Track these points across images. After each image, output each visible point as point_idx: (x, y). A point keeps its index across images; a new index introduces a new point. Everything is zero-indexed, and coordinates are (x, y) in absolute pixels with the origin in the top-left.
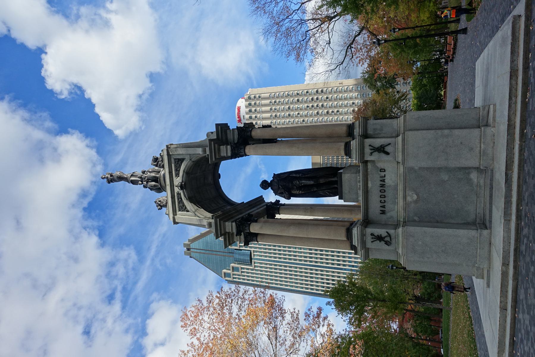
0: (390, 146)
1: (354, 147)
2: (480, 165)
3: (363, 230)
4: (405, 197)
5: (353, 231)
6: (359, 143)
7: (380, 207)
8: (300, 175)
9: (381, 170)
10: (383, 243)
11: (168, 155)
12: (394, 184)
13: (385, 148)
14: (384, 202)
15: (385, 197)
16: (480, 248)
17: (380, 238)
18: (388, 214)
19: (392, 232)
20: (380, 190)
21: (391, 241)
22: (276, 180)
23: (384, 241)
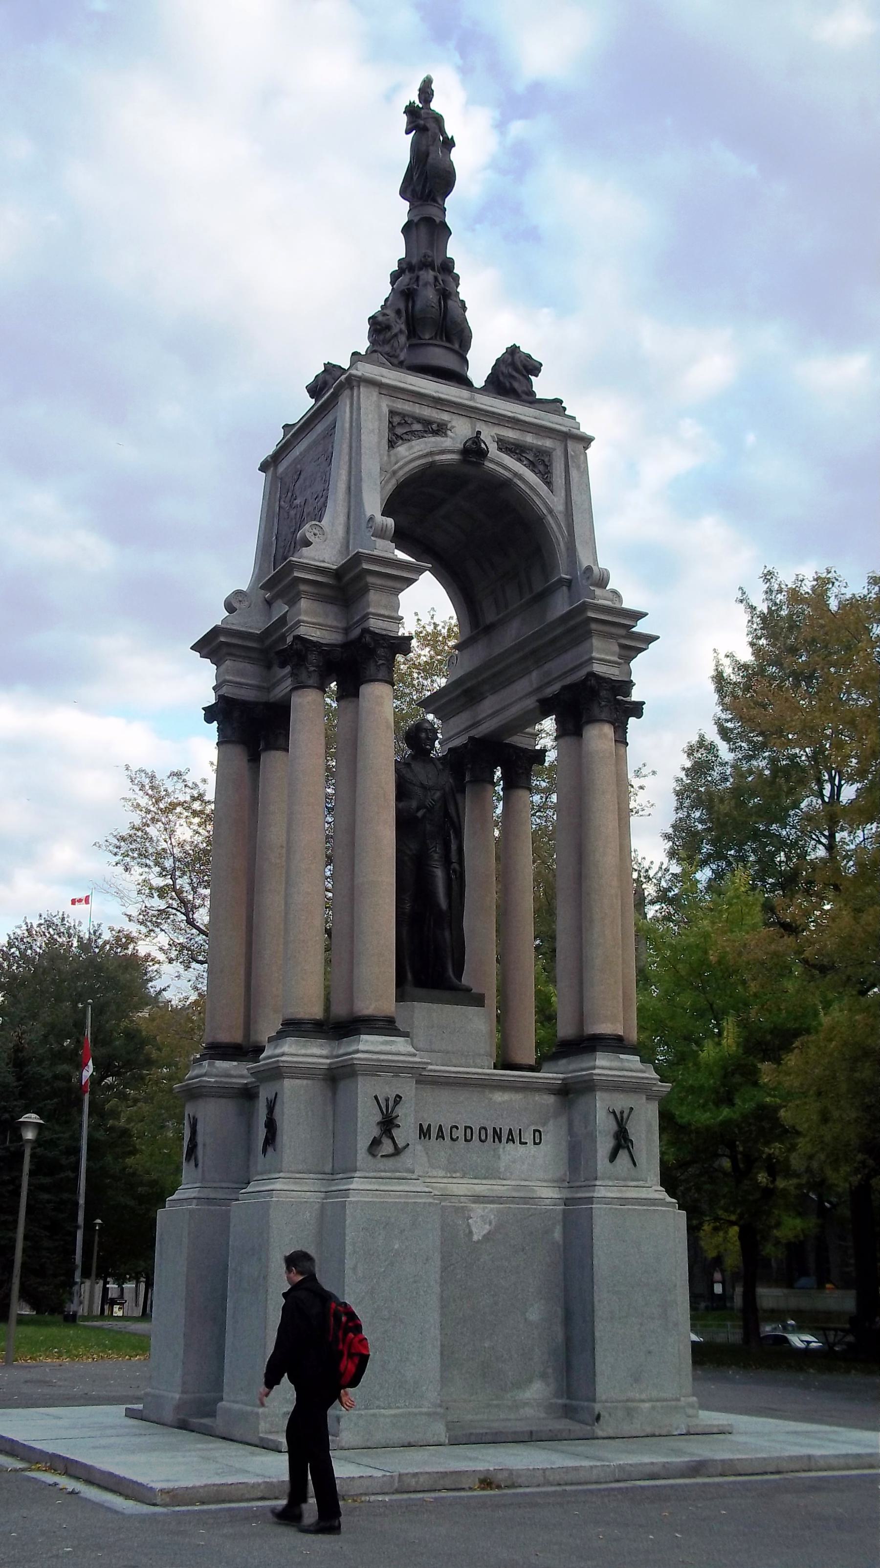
0: (631, 1165)
1: (626, 1065)
3: (413, 1071)
4: (478, 1199)
7: (440, 1126)
9: (537, 1134)
10: (376, 1132)
12: (502, 1169)
14: (454, 1137)
15: (466, 1140)
16: (395, 1416)
17: (388, 1124)
18: (419, 1147)
19: (406, 1159)
23: (381, 1136)
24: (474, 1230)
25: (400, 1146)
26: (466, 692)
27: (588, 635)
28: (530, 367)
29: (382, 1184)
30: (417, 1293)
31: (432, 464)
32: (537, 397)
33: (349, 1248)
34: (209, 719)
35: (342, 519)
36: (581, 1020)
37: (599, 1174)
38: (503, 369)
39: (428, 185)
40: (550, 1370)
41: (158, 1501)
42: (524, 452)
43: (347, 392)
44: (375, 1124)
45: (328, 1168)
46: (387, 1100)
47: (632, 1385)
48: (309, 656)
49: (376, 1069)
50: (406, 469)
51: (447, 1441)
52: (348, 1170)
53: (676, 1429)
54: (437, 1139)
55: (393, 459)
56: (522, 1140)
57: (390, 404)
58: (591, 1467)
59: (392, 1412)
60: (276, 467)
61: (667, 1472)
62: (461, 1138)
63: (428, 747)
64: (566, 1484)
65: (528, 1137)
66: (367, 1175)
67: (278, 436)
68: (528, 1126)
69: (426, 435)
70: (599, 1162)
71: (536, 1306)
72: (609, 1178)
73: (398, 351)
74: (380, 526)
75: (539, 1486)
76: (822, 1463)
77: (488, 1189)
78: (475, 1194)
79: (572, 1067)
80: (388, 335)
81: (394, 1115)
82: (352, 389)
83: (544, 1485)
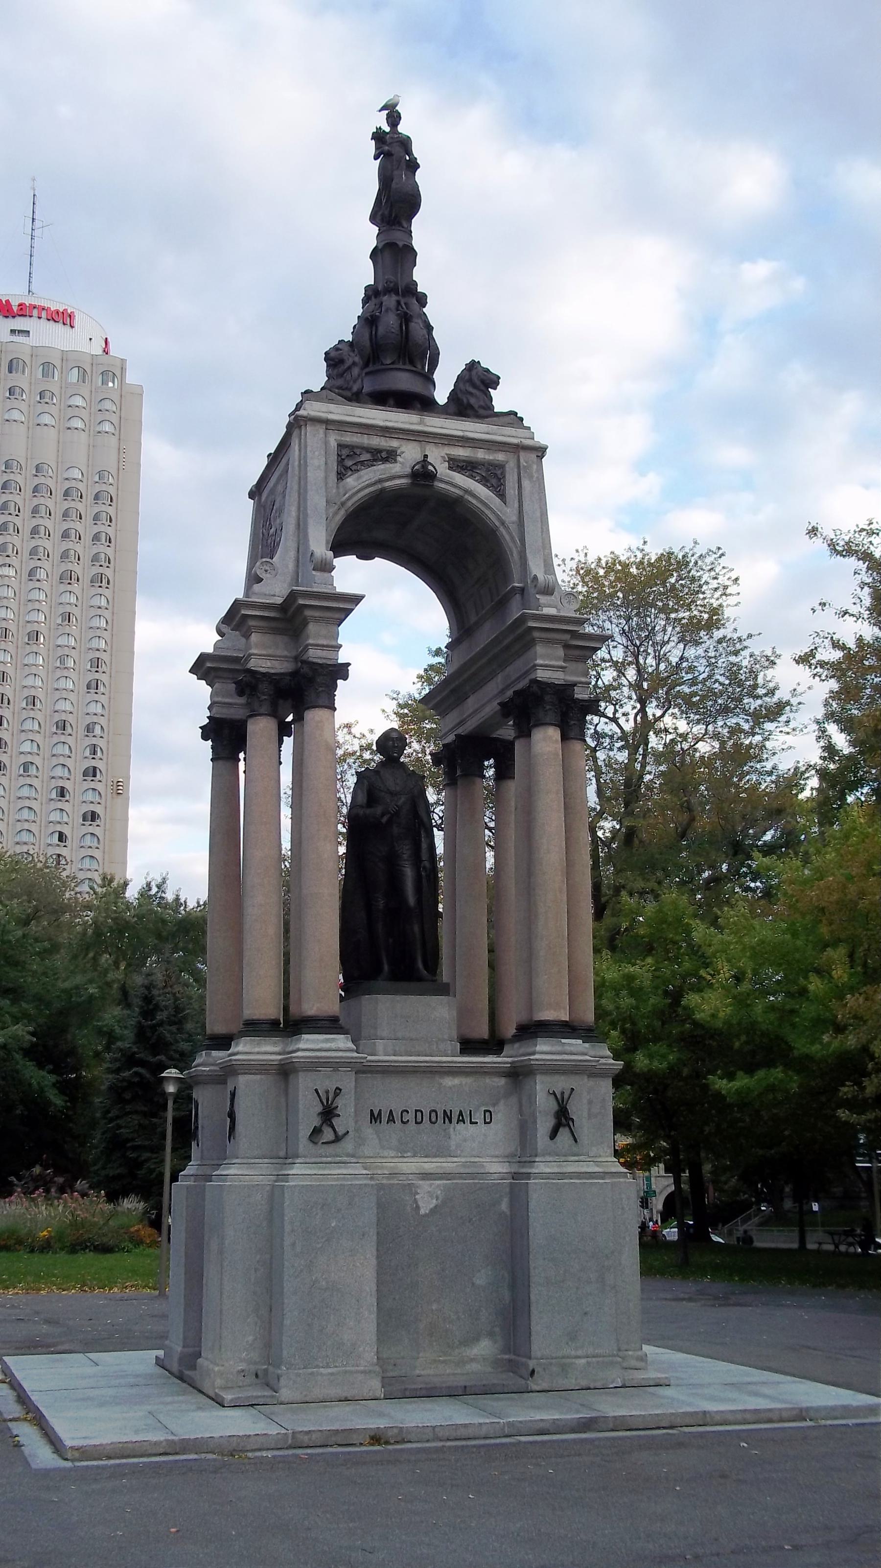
1: (568, 1048)
2: (537, 1359)
3: (351, 1065)
4: (426, 1176)
7: (391, 1111)
8: (427, 864)
9: (488, 1114)
10: (316, 1122)
11: (517, 448)
15: (416, 1123)
16: (332, 1374)
17: (328, 1114)
19: (348, 1145)
23: (322, 1125)
24: (420, 1204)
25: (340, 1134)
26: (453, 691)
27: (532, 643)
28: (488, 381)
29: (320, 1168)
30: (353, 1265)
31: (382, 490)
32: (495, 411)
33: (288, 1228)
34: (205, 737)
35: (292, 554)
36: (530, 1005)
37: (539, 1151)
38: (461, 385)
39: (394, 210)
40: (497, 1329)
41: (69, 1456)
42: (476, 468)
43: (296, 433)
44: (315, 1115)
45: (282, 1153)
46: (327, 1092)
47: (567, 1343)
48: (260, 686)
49: (314, 1065)
50: (355, 499)
51: (382, 1396)
52: (288, 1157)
53: (612, 1382)
55: (341, 491)
57: (339, 438)
58: (480, 1424)
59: (330, 1370)
60: (260, 495)
61: (557, 1428)
63: (395, 755)
64: (448, 1440)
65: (478, 1117)
66: (308, 1160)
67: (265, 462)
69: (375, 463)
70: (539, 1140)
71: (483, 1271)
72: (549, 1154)
73: (351, 383)
74: (320, 561)
75: (428, 1441)
76: (718, 1418)
77: (437, 1167)
78: (423, 1171)
79: (522, 1051)
80: (343, 368)
81: (334, 1105)
82: (300, 427)
83: (433, 1440)
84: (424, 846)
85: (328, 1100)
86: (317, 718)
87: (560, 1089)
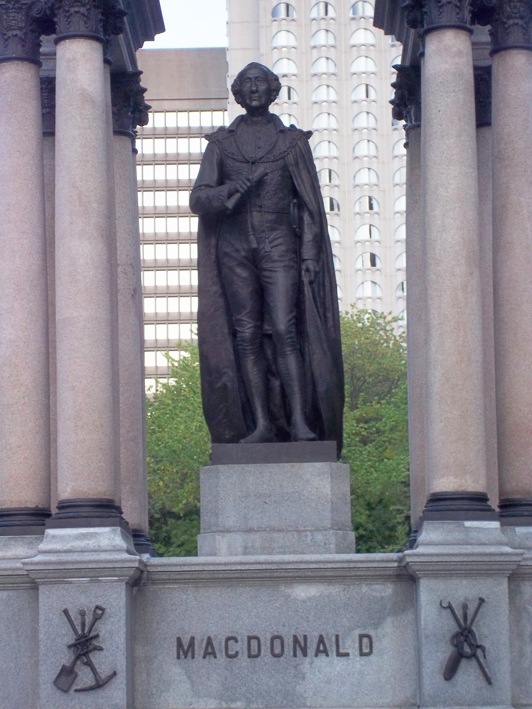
0: (484, 683)
1: (473, 534)
5: (107, 529)
6: (493, 559)
7: (209, 639)
8: (311, 265)
9: (365, 640)
13: (474, 662)
15: (250, 656)
20: (283, 632)
21: (76, 691)
22: (282, 146)
23: (74, 663)
25: (103, 677)
54: (204, 657)
56: (341, 651)
62: (243, 653)
68: (351, 630)
81: (92, 634)
84: (308, 236)
85: (83, 625)
86: (69, 55)
87: (462, 599)
